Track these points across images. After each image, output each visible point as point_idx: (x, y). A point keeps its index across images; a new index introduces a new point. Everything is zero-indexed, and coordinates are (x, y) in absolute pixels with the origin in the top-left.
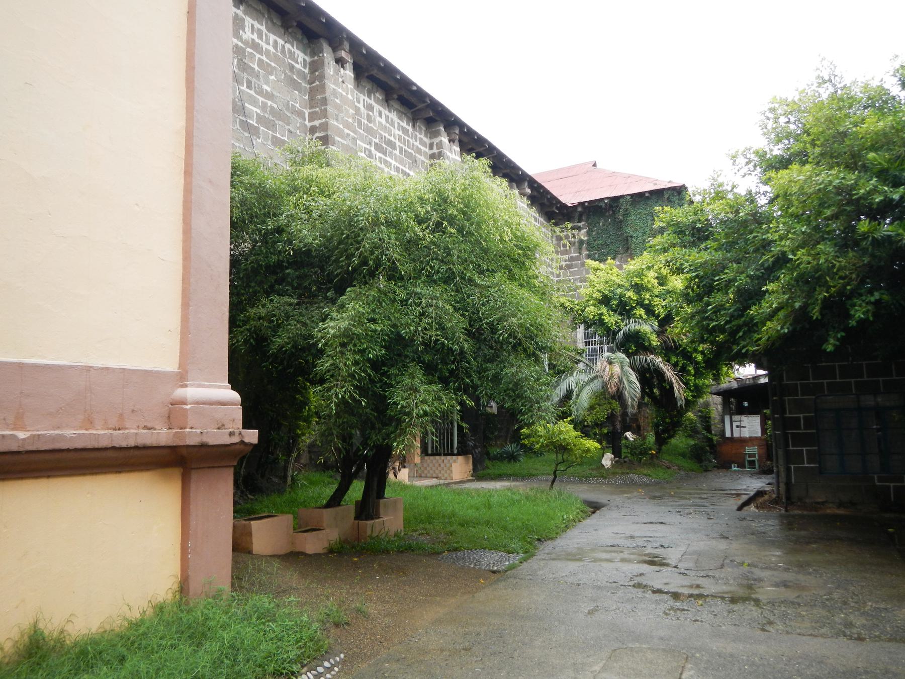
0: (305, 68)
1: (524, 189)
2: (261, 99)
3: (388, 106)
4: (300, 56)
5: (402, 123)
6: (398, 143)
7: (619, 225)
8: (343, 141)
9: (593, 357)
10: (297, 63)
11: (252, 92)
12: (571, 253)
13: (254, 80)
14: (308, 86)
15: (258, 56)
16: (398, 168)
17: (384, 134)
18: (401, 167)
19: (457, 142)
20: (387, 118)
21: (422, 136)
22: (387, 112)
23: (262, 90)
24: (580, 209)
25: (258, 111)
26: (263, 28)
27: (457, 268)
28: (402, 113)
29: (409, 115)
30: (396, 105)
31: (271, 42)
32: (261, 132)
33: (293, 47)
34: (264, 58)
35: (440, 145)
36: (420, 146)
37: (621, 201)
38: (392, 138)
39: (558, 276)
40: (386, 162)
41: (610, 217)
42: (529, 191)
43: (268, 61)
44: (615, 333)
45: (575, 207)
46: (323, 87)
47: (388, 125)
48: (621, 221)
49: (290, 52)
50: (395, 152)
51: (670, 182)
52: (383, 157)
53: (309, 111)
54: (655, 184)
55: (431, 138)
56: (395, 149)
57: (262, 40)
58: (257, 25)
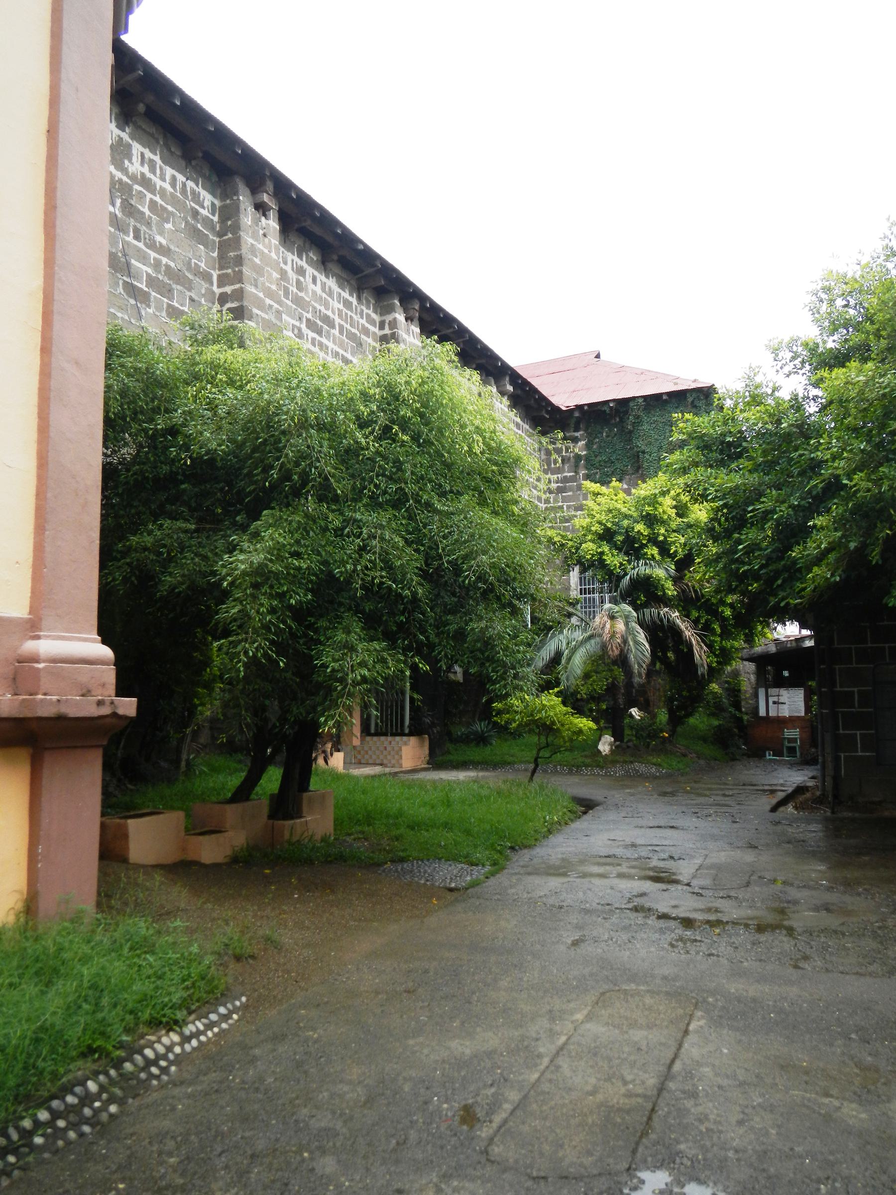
0: (214, 215)
1: (505, 385)
2: (153, 255)
3: (325, 270)
4: (207, 198)
5: (343, 294)
6: (338, 321)
7: (628, 436)
9: (591, 608)
10: (203, 207)
11: (141, 245)
12: (564, 472)
13: (143, 228)
14: (217, 240)
15: (149, 196)
16: (337, 354)
17: (318, 307)
18: (341, 352)
19: (416, 321)
20: (323, 285)
21: (370, 312)
23: (155, 242)
24: (577, 414)
25: (150, 271)
26: (157, 159)
27: (411, 488)
28: (341, 277)
29: (353, 282)
30: (337, 269)
31: (168, 178)
32: (152, 299)
33: (197, 186)
34: (157, 199)
35: (393, 324)
36: (367, 325)
37: (631, 404)
38: (329, 313)
39: (547, 501)
40: (321, 345)
41: (616, 425)
42: (510, 388)
43: (163, 203)
44: (620, 578)
45: (570, 412)
46: (237, 242)
47: (324, 295)
48: (631, 432)
49: (193, 192)
50: (333, 331)
51: (695, 381)
53: (218, 272)
54: (676, 384)
55: (381, 315)
56: (333, 327)
58: (148, 154)
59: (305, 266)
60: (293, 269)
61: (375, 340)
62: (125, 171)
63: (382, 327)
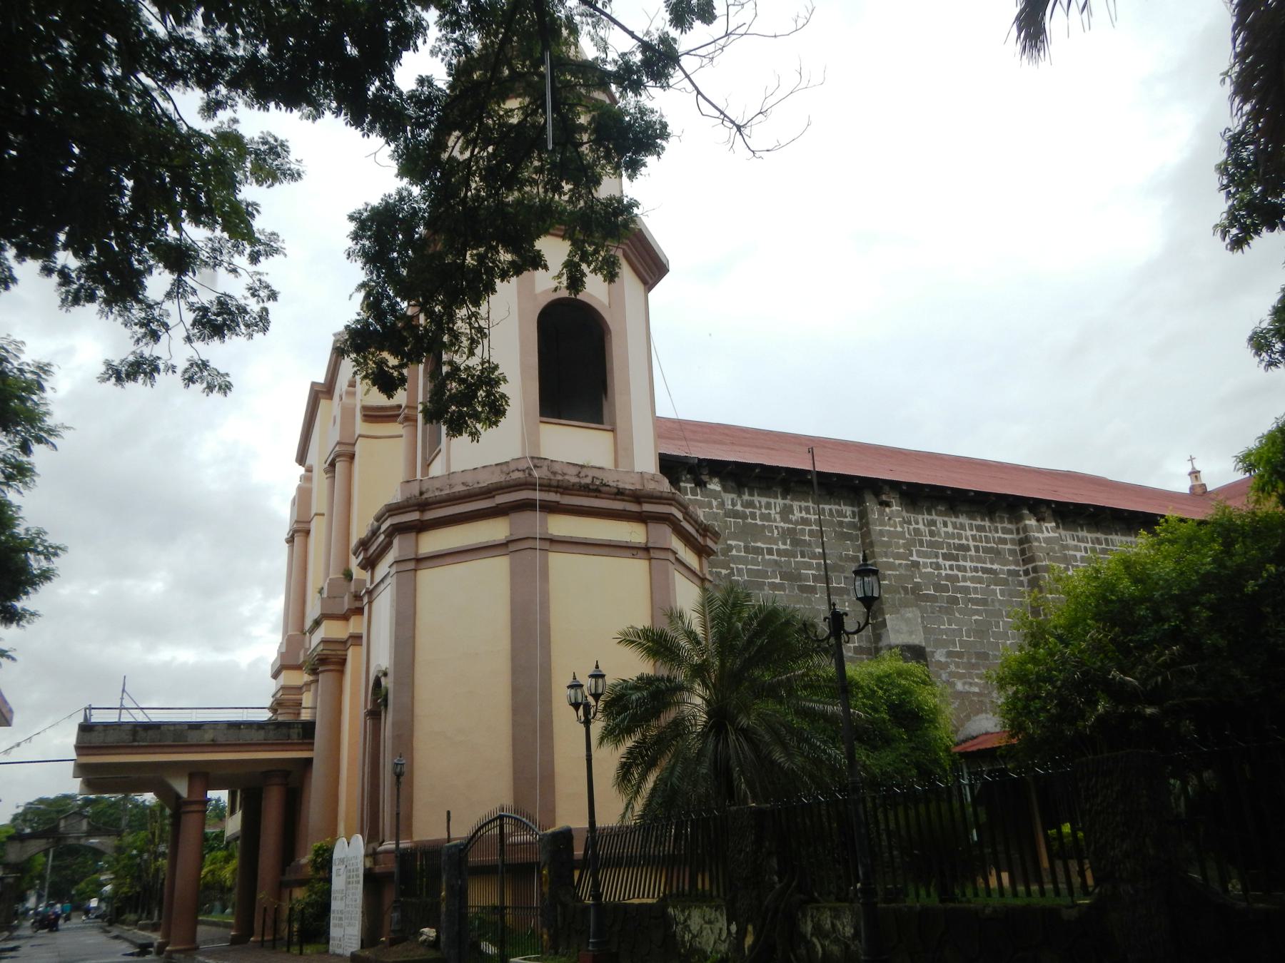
2: (814, 561)
4: (848, 510)
5: (974, 522)
6: (971, 543)
8: (894, 573)
10: (847, 517)
11: (806, 559)
13: (806, 549)
14: (859, 533)
17: (952, 541)
18: (979, 565)
22: (954, 519)
26: (810, 504)
35: (1025, 529)
38: (964, 542)
40: (959, 568)
49: (837, 511)
50: (970, 553)
52: (954, 563)
57: (810, 514)
58: (803, 504)
59: (934, 517)
60: (924, 525)
61: (1012, 544)
62: (790, 522)
63: (1018, 533)
